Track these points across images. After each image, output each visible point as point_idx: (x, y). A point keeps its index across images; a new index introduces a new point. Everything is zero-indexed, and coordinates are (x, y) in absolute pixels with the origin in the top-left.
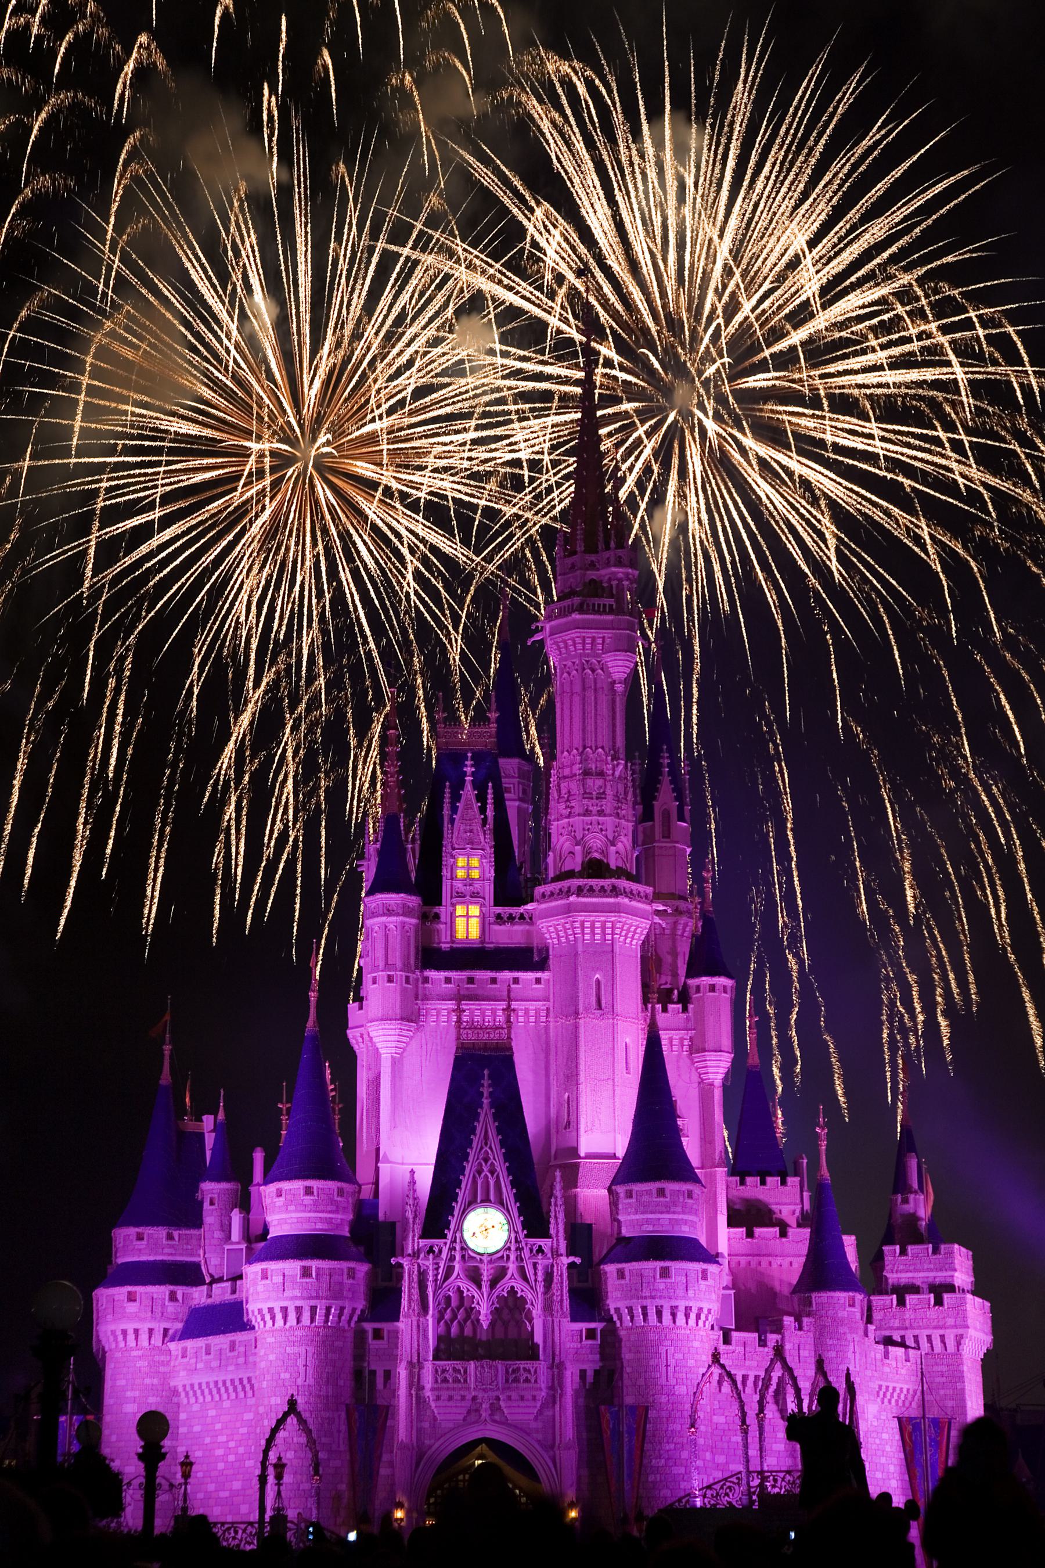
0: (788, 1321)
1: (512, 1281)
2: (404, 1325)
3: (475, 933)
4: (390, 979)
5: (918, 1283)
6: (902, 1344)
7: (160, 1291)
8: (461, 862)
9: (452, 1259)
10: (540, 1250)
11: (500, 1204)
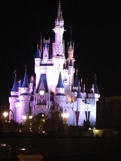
1: (44, 97)
2: (34, 102)
11: (44, 90)
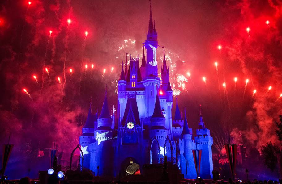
0: (180, 139)
3: (134, 86)
4: (121, 92)
5: (202, 135)
6: (199, 143)
7: (87, 137)
8: (133, 76)
9: (125, 129)
10: (139, 128)
